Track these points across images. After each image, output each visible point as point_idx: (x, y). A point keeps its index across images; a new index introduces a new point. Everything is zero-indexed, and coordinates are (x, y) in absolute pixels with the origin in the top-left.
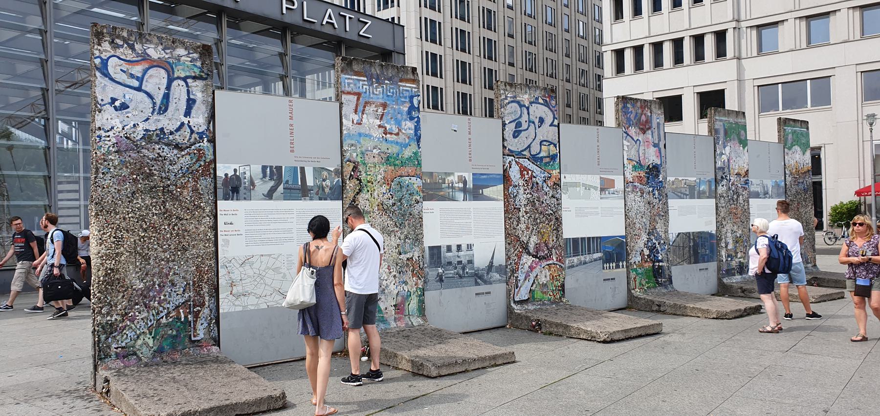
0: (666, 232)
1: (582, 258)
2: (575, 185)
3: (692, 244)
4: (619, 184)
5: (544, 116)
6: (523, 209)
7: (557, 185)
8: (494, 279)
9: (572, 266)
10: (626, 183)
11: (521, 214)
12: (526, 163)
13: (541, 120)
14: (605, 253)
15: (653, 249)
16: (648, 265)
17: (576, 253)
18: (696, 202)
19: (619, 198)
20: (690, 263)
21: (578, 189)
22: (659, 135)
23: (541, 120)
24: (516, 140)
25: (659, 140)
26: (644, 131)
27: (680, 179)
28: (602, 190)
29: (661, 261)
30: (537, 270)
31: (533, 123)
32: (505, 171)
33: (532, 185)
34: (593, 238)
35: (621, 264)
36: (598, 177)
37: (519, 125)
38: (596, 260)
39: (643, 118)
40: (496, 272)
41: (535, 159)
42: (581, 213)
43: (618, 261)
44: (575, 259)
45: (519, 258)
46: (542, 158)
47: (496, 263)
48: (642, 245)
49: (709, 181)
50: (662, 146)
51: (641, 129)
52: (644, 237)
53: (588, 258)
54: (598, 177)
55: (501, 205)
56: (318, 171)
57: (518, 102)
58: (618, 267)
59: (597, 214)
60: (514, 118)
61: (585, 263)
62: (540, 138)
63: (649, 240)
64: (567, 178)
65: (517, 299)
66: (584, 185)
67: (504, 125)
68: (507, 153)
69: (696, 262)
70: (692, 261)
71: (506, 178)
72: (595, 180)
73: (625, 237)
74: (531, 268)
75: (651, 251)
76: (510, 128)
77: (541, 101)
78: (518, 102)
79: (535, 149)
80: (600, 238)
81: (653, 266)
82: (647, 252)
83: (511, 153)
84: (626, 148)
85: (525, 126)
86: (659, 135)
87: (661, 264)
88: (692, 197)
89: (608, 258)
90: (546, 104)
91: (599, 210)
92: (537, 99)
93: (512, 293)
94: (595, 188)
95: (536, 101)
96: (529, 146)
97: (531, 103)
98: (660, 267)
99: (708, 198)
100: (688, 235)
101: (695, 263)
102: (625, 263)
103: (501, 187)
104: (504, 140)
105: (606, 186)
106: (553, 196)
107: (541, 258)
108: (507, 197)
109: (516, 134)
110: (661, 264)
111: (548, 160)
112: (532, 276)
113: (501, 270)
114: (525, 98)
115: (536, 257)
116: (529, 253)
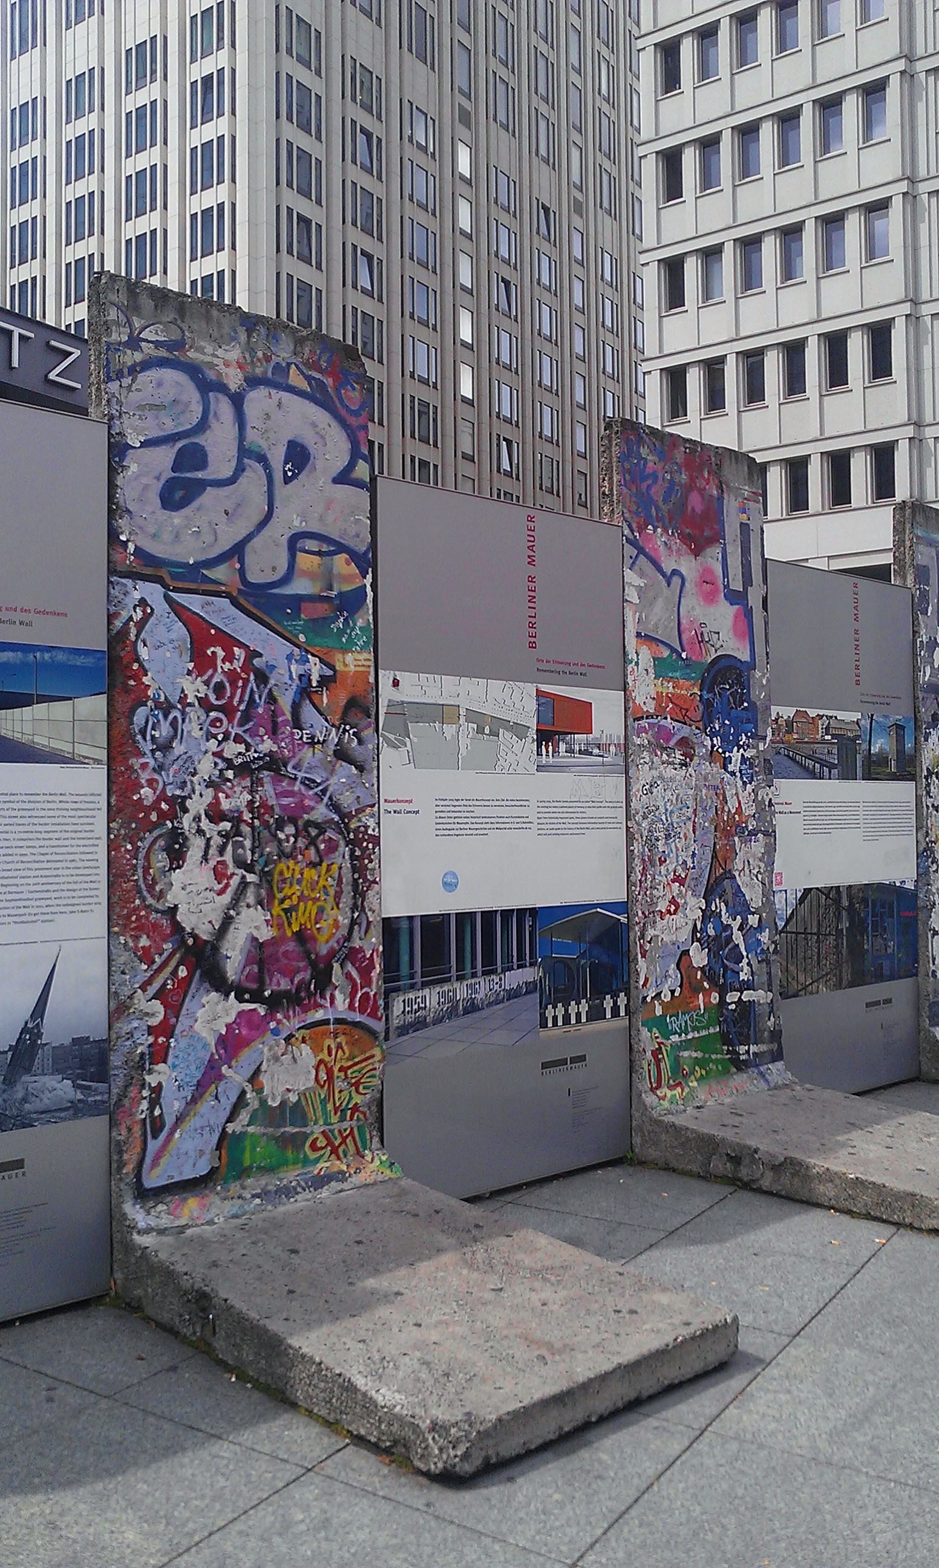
0: (768, 894)
1: (461, 991)
2: (442, 713)
3: (845, 924)
5: (309, 439)
6: (197, 805)
7: (359, 708)
8: (46, 1100)
9: (420, 1024)
10: (632, 715)
11: (187, 821)
12: (221, 613)
13: (298, 456)
14: (553, 968)
15: (719, 946)
16: (706, 1000)
17: (435, 970)
18: (860, 790)
19: (606, 769)
20: (839, 986)
21: (449, 730)
22: (746, 566)
23: (298, 456)
24: (177, 518)
25: (747, 581)
26: (697, 546)
27: (812, 713)
28: (545, 737)
29: (748, 986)
30: (263, 1049)
31: (262, 459)
32: (118, 639)
33: (241, 700)
34: (506, 914)
35: (608, 1003)
36: (531, 689)
37: (192, 457)
38: (513, 994)
39: (695, 502)
40: (56, 1071)
42: (454, 819)
43: (599, 992)
44: (432, 998)
45: (174, 1008)
46: (298, 601)
47: (56, 1031)
48: (685, 934)
49: (900, 728)
50: (754, 599)
51: (686, 539)
52: (694, 907)
53: (484, 987)
54: (531, 689)
55: (95, 779)
57: (193, 371)
58: (596, 1014)
59: (523, 823)
60: (170, 427)
61: (472, 1008)
62: (291, 518)
63: (708, 915)
64: (404, 687)
65: (153, 1179)
66: (473, 716)
67: (117, 450)
69: (859, 980)
70: (846, 976)
71: (115, 670)
72: (518, 702)
73: (622, 907)
74: (230, 1044)
75: (713, 954)
76: (149, 469)
77: (295, 379)
78: (193, 371)
79: (265, 562)
80: (533, 912)
81: (722, 1002)
82: (699, 958)
83: (149, 568)
84: (632, 595)
85: (221, 464)
86: (746, 566)
87: (746, 996)
88: (848, 774)
89: (561, 986)
90: (319, 397)
91: (531, 812)
92: (282, 370)
93: (131, 1157)
94: (519, 730)
95: (276, 380)
96: (238, 551)
97: (253, 382)
98: (746, 1008)
99: (894, 777)
100: (832, 894)
101: (851, 985)
102: (622, 1000)
103: (93, 707)
104: (114, 510)
105: (558, 725)
106: (342, 754)
107: (274, 1003)
108: (120, 748)
109: (178, 493)
110: (746, 996)
111: (322, 610)
112: (235, 1076)
113: (89, 1060)
114: (226, 360)
115: (256, 997)
116: (220, 984)
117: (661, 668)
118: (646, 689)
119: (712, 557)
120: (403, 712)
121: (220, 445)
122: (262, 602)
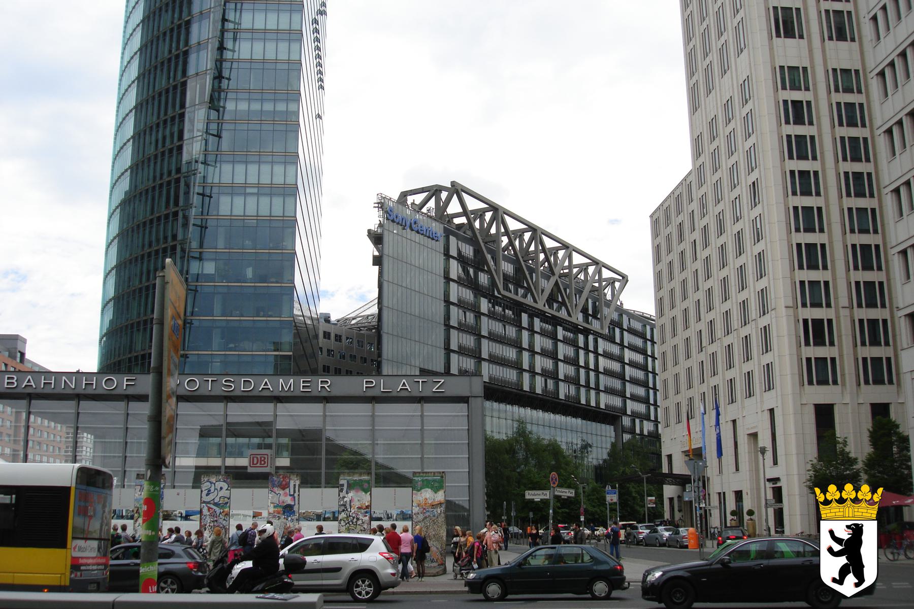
4: (265, 514)
7: (227, 514)
10: (269, 514)
12: (212, 506)
13: (221, 488)
25: (295, 492)
26: (284, 489)
41: (216, 504)
49: (334, 513)
56: (127, 511)
68: (202, 502)
71: (201, 512)
76: (205, 493)
79: (217, 500)
83: (204, 502)
108: (201, 519)
109: (207, 495)
114: (213, 480)
117: (275, 507)
118: (272, 510)
119: (287, 490)
120: (233, 515)
121: (212, 489)
122: (216, 504)
